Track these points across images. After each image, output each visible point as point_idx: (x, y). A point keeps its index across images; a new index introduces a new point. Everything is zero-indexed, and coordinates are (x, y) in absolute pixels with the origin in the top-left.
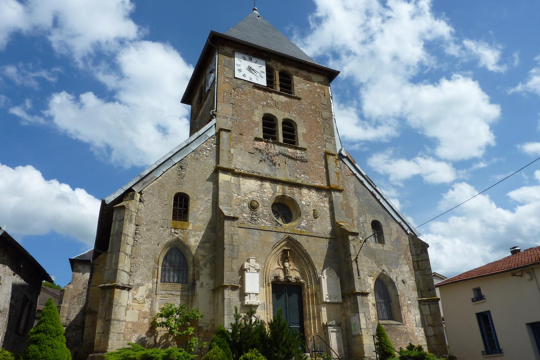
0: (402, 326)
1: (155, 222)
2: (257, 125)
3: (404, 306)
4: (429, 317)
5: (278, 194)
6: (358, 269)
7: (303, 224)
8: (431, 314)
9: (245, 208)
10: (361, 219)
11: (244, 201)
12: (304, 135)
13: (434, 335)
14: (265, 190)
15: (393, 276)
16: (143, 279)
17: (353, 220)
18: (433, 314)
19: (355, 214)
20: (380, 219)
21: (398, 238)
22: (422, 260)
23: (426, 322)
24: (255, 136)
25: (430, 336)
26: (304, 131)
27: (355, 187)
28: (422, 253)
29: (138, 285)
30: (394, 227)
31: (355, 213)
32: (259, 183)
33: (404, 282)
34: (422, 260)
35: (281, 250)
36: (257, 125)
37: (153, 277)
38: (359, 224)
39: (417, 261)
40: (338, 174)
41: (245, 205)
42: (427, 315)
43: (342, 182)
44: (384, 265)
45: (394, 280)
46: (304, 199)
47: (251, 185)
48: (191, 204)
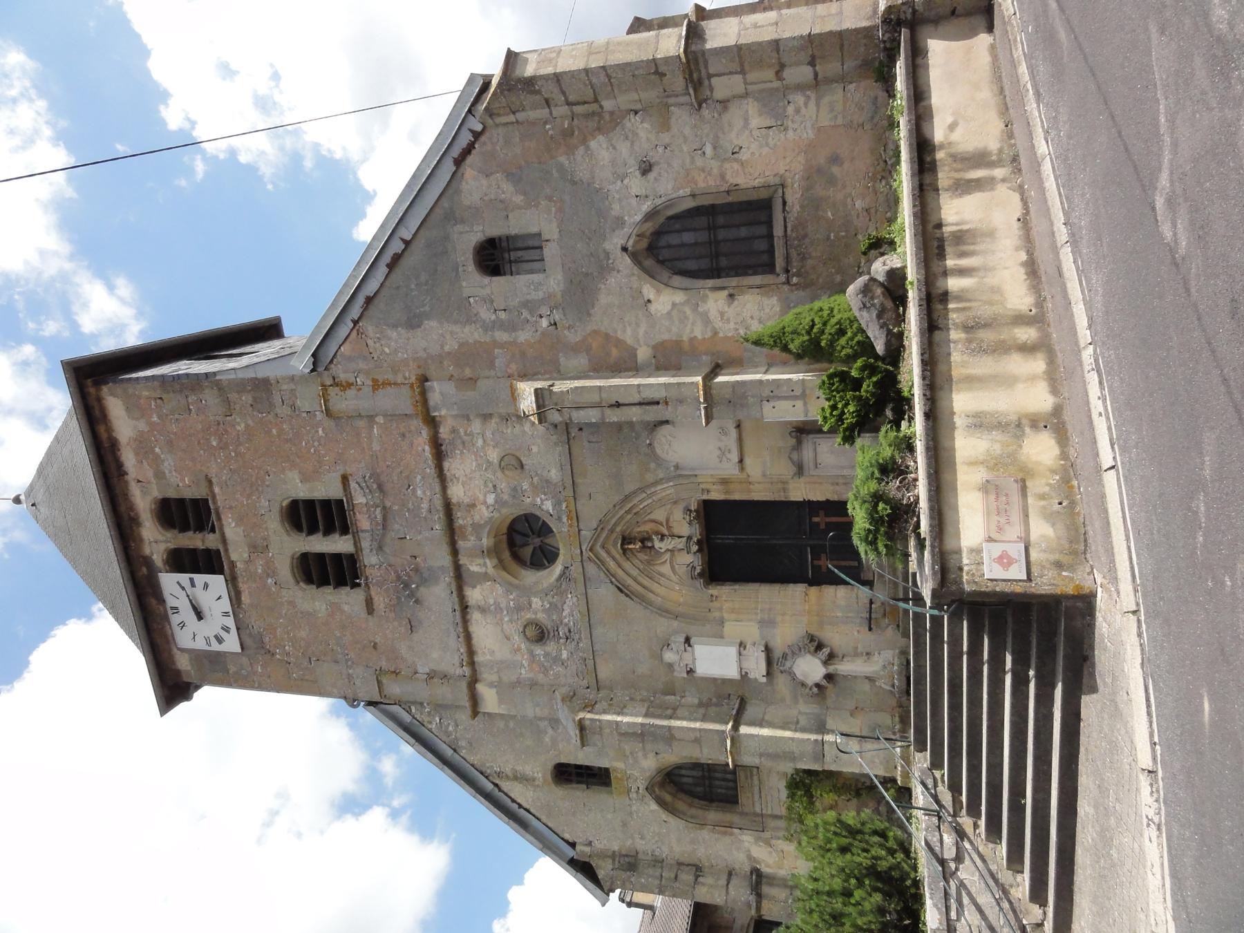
0: (788, 192)
1: (624, 824)
2: (335, 608)
3: (723, 176)
4: (751, 77)
5: (491, 570)
6: (640, 404)
7: (548, 506)
8: (742, 72)
9: (547, 655)
10: (486, 315)
11: (531, 653)
12: (305, 479)
13: (812, 63)
14: (491, 601)
15: (634, 214)
16: (738, 849)
17: (496, 345)
18: (742, 65)
19: (476, 336)
20: (468, 238)
21: (509, 176)
22: (564, 93)
23: (769, 85)
24: (364, 614)
25: (816, 75)
26: (293, 476)
27: (395, 326)
28: (539, 92)
29: (750, 857)
30: (474, 185)
31: (471, 334)
32: (475, 616)
33: (646, 168)
34: (564, 93)
35: (627, 565)
36: (335, 608)
37: (732, 834)
38: (502, 326)
39: (569, 104)
40: (376, 385)
41: (539, 651)
42: (746, 83)
43: (395, 371)
44: (607, 246)
45: (646, 207)
46: (481, 497)
47: (485, 633)
48: (563, 760)
